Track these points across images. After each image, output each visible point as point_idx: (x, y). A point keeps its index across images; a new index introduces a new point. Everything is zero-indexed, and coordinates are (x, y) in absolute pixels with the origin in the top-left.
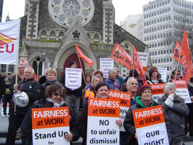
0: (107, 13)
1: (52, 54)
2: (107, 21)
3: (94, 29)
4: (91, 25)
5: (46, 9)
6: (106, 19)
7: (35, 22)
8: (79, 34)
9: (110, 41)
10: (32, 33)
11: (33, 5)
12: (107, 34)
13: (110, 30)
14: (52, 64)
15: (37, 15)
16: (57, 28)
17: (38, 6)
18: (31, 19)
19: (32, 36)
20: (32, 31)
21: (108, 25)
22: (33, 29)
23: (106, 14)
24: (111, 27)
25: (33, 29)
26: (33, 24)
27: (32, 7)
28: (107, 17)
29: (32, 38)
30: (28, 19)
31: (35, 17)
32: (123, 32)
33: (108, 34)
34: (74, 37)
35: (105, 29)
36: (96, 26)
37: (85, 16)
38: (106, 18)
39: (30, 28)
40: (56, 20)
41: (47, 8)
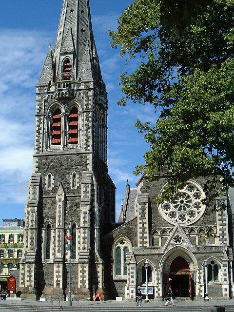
1: (156, 260)
8: (181, 238)
9: (225, 234)
10: (143, 235)
12: (221, 227)
13: (224, 222)
14: (157, 268)
15: (147, 216)
17: (147, 206)
20: (143, 233)
22: (143, 231)
24: (225, 220)
25: (143, 231)
26: (143, 225)
29: (143, 240)
30: (139, 221)
35: (218, 222)
37: (198, 209)
39: (141, 230)
40: (167, 218)
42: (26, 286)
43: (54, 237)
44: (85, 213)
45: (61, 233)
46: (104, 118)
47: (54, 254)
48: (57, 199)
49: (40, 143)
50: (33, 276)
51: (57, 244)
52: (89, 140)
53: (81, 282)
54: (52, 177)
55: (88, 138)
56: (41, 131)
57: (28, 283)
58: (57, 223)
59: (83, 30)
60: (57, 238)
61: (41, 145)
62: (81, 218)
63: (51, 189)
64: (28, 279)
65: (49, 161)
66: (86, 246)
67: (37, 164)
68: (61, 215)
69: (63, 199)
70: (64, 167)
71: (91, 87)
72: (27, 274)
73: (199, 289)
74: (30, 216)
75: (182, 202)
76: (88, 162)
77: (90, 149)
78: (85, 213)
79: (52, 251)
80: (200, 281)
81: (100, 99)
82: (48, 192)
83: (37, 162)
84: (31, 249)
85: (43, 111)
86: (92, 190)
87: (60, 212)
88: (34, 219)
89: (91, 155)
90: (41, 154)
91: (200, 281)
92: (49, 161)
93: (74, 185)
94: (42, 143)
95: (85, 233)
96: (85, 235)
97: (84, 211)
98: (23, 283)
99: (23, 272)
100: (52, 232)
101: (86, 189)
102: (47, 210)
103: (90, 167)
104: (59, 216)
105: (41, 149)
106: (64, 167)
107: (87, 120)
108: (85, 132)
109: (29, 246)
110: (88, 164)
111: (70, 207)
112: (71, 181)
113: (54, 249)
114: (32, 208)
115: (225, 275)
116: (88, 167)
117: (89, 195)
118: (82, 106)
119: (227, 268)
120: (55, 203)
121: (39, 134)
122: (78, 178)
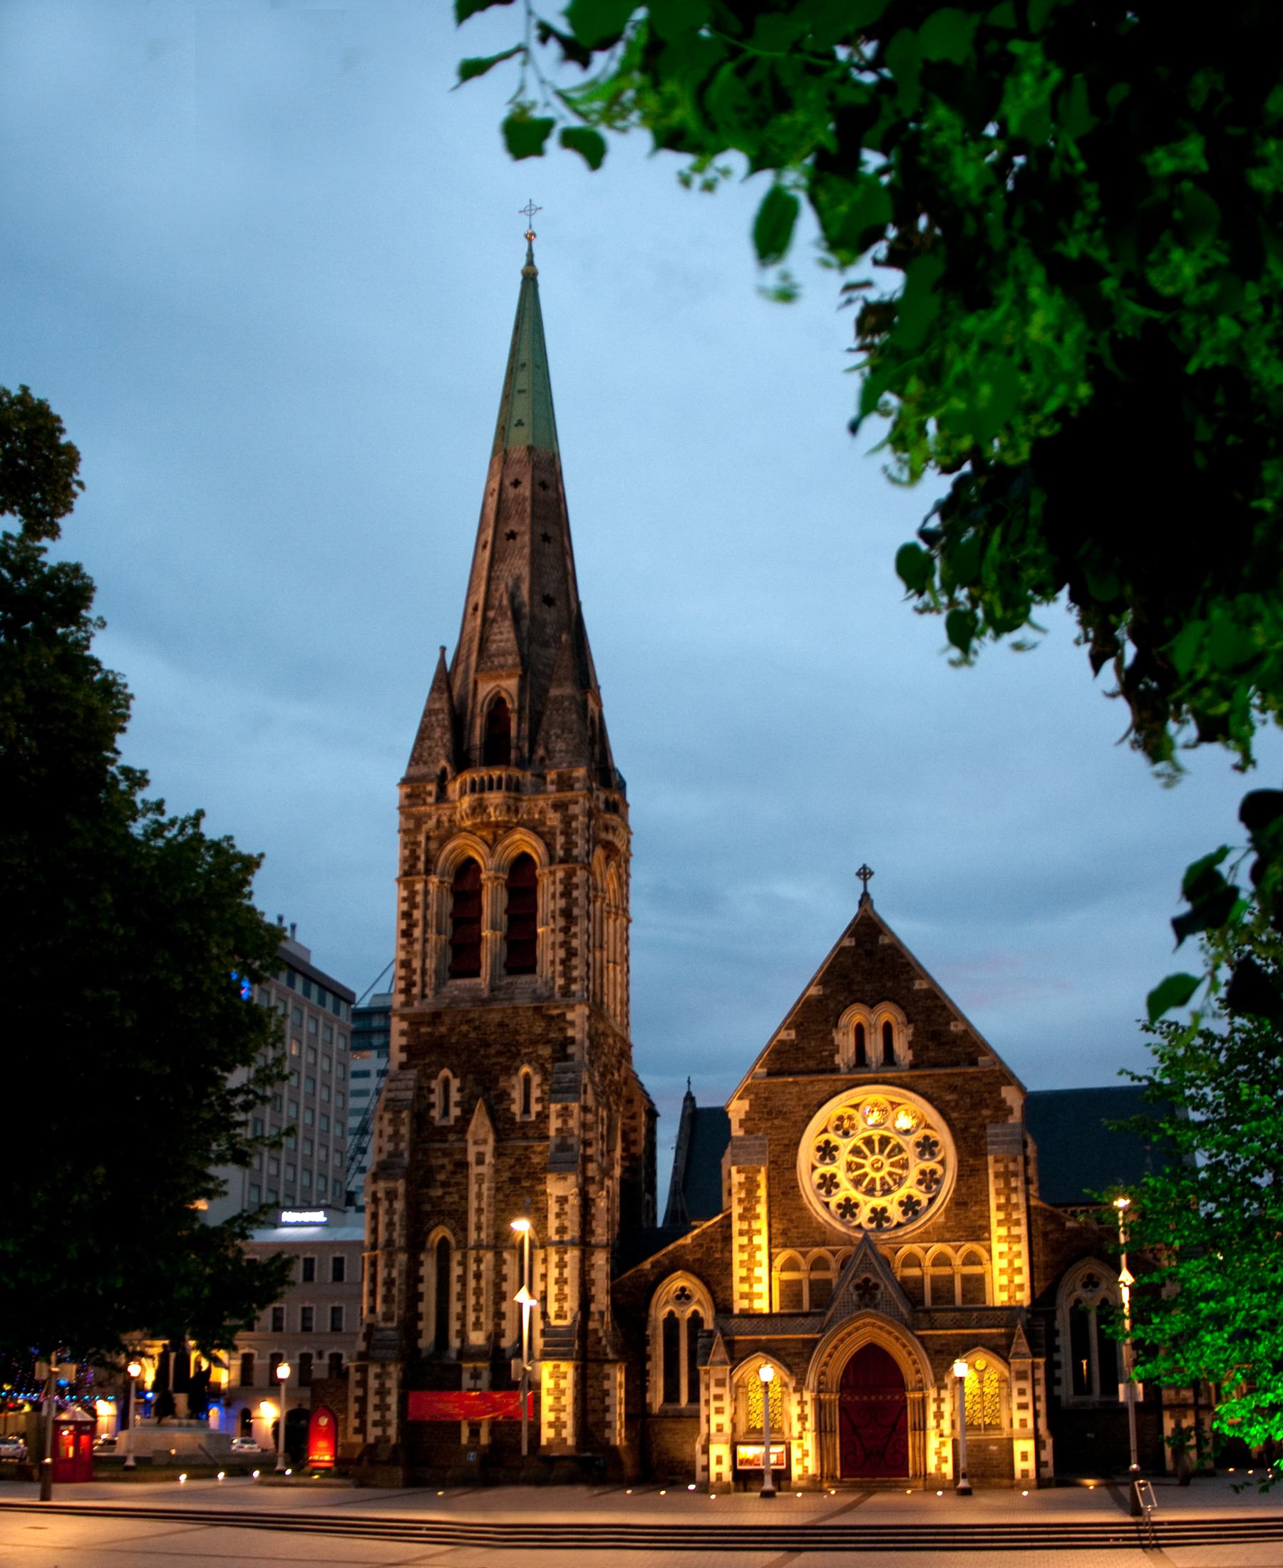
0: (1002, 1170)
2: (1002, 1200)
3: (960, 1234)
5: (791, 1180)
6: (998, 1193)
7: (759, 1232)
11: (746, 1178)
15: (762, 1209)
16: (834, 1245)
18: (745, 1226)
19: (753, 1280)
21: (1006, 1215)
23: (997, 1176)
27: (744, 1183)
28: (1002, 1186)
29: (751, 1286)
30: (737, 1226)
31: (757, 1217)
32: (1071, 1230)
33: (1010, 1249)
34: (861, 1297)
36: (967, 1223)
38: (996, 1190)
39: (745, 1256)
41: (796, 1180)
42: (371, 1440)
43: (462, 1279)
44: (562, 1200)
45: (483, 1267)
46: (621, 886)
47: (462, 1334)
48: (471, 1158)
49: (414, 972)
50: (394, 1407)
51: (472, 1300)
52: (575, 961)
53: (551, 1425)
55: (571, 953)
56: (417, 932)
57: (378, 1431)
58: (473, 1236)
60: (472, 1283)
61: (417, 978)
62: (551, 1217)
63: (451, 1121)
64: (376, 1416)
66: (567, 1306)
67: (404, 1041)
68: (484, 1205)
69: (489, 1159)
70: (493, 1052)
72: (373, 1400)
73: (938, 1453)
74: (381, 1212)
76: (570, 1033)
78: (562, 1200)
79: (454, 1325)
80: (938, 1426)
81: (606, 828)
82: (442, 1132)
83: (403, 1033)
84: (388, 1317)
85: (421, 866)
87: (479, 1196)
88: (396, 1218)
91: (938, 1426)
92: (443, 1029)
93: (526, 1110)
94: (419, 971)
95: (561, 1265)
96: (561, 1274)
97: (561, 1193)
98: (361, 1430)
99: (359, 1392)
100: (456, 1257)
101: (565, 1122)
102: (439, 1192)
104: (479, 1211)
105: (415, 991)
107: (566, 894)
108: (560, 937)
109: (380, 1308)
111: (515, 1180)
112: (517, 1094)
113: (462, 1317)
114: (391, 1185)
115: (1022, 1407)
116: (571, 1050)
118: (550, 847)
119: (1026, 1385)
120: (463, 1166)
122: (539, 1085)
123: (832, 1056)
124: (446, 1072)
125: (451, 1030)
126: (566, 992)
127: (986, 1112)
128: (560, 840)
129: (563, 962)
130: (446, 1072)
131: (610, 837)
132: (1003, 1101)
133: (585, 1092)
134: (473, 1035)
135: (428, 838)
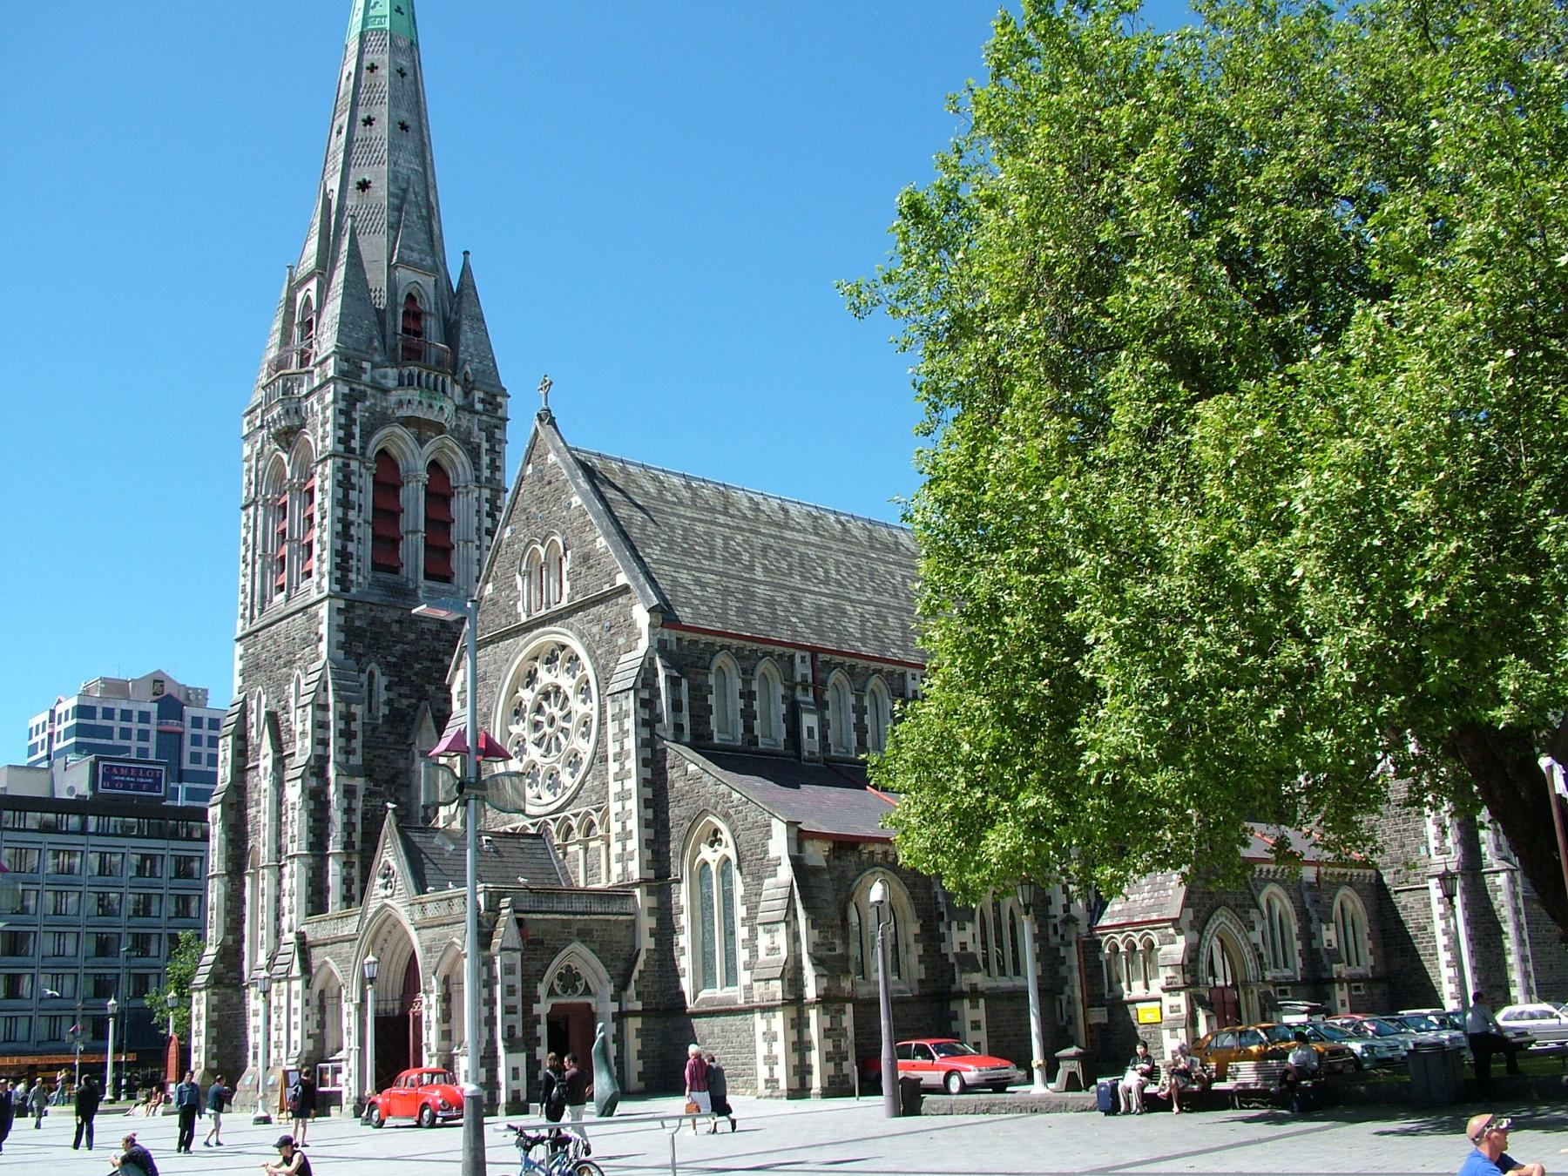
2: (618, 749)
4: (594, 778)
35: (614, 787)
54: (264, 698)
59: (364, 186)
65: (259, 647)
69: (270, 770)
70: (282, 661)
71: (331, 373)
75: (552, 721)
77: (325, 582)
86: (321, 725)
89: (326, 603)
90: (248, 629)
103: (323, 647)
106: (282, 661)
110: (320, 639)
117: (308, 742)
121: (247, 565)
123: (515, 604)
124: (260, 688)
125: (263, 648)
126: (319, 585)
127: (621, 641)
128: (320, 431)
129: (319, 556)
130: (260, 688)
131: (410, 413)
132: (632, 625)
133: (326, 689)
134: (273, 648)
135: (258, 460)
